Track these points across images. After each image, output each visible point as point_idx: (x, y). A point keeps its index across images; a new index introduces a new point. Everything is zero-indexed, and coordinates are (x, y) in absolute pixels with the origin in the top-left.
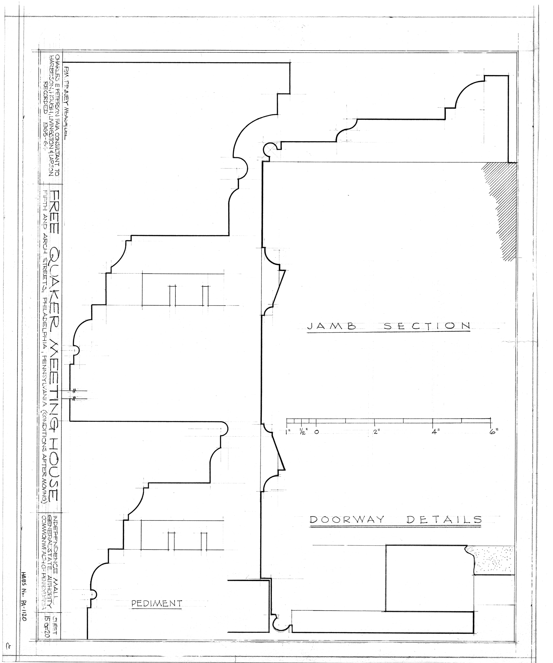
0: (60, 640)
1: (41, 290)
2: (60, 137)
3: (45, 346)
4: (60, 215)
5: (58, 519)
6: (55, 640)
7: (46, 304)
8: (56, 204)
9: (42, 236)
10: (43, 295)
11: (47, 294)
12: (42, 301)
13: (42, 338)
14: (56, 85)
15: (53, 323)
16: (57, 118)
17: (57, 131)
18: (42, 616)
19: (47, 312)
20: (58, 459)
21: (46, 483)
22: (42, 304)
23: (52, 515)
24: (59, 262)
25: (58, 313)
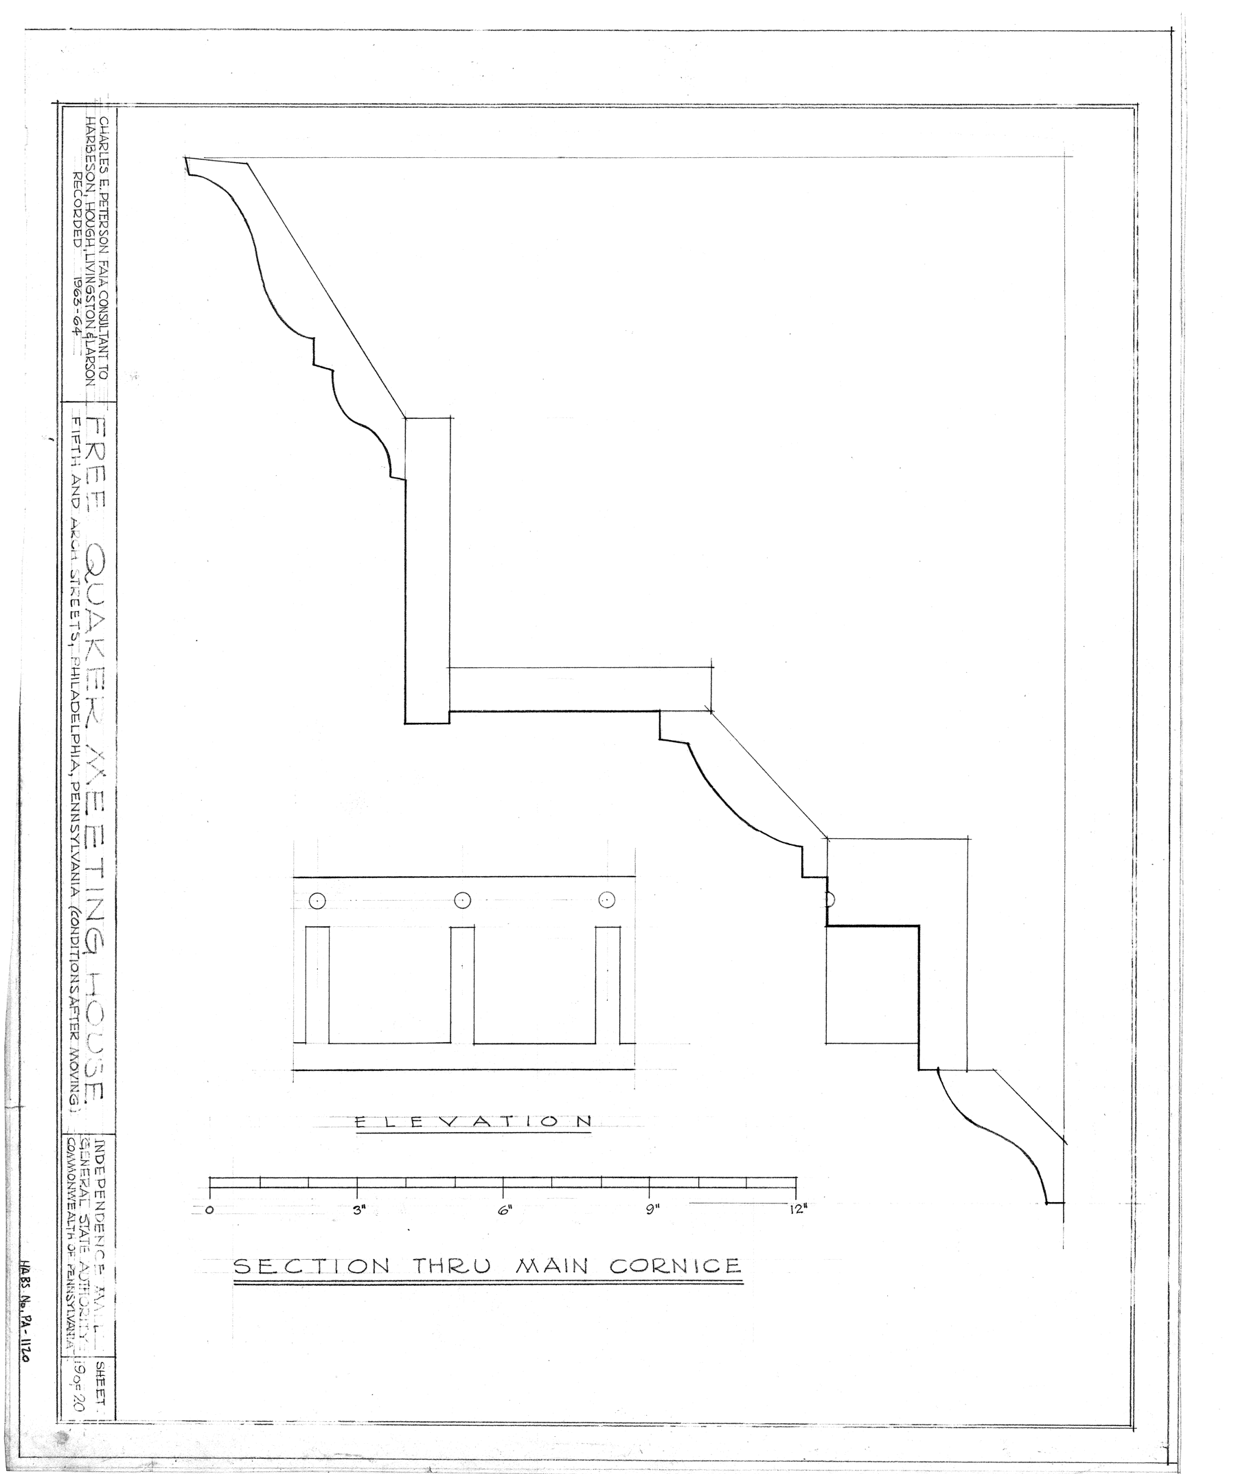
17: (102, 288)
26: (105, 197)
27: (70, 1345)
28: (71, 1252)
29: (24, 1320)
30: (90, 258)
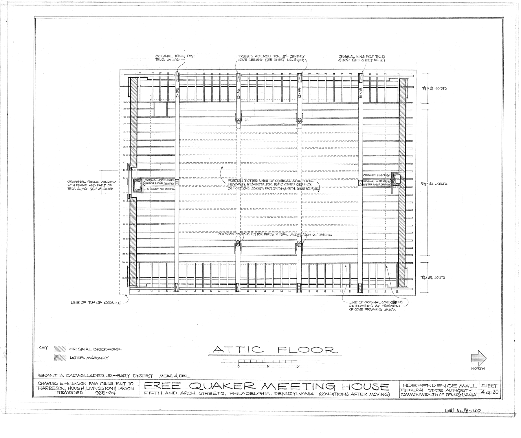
0: (502, 382)
1: (224, 396)
2: (103, 381)
3: (268, 393)
4: (236, 382)
5: (405, 383)
6: (501, 385)
7: (235, 393)
8: (156, 384)
9: (182, 395)
10: (228, 395)
11: (227, 391)
12: (232, 395)
13: (307, 396)
14: (61, 384)
15: (250, 387)
16: (88, 384)
17: (99, 384)
18: (482, 396)
19: (241, 392)
20: (357, 384)
21: (373, 393)
22: (235, 396)
23: (401, 388)
24: (202, 382)
25: (288, 384)
26: (66, 383)
27: (475, 395)
28: (442, 395)
29: (465, 411)
30: (88, 388)
